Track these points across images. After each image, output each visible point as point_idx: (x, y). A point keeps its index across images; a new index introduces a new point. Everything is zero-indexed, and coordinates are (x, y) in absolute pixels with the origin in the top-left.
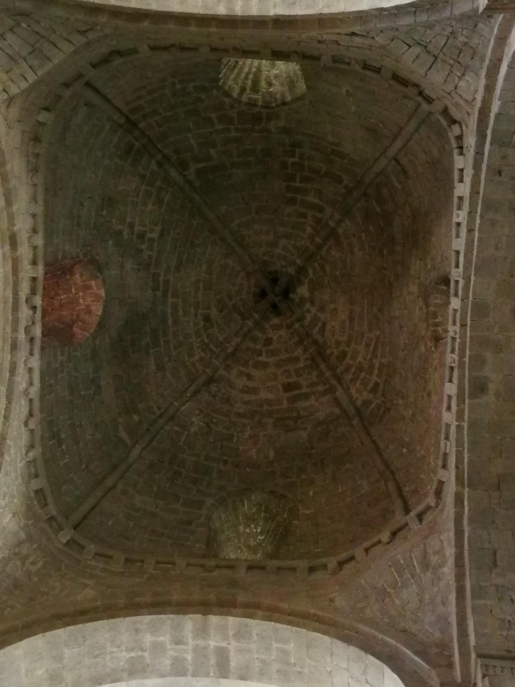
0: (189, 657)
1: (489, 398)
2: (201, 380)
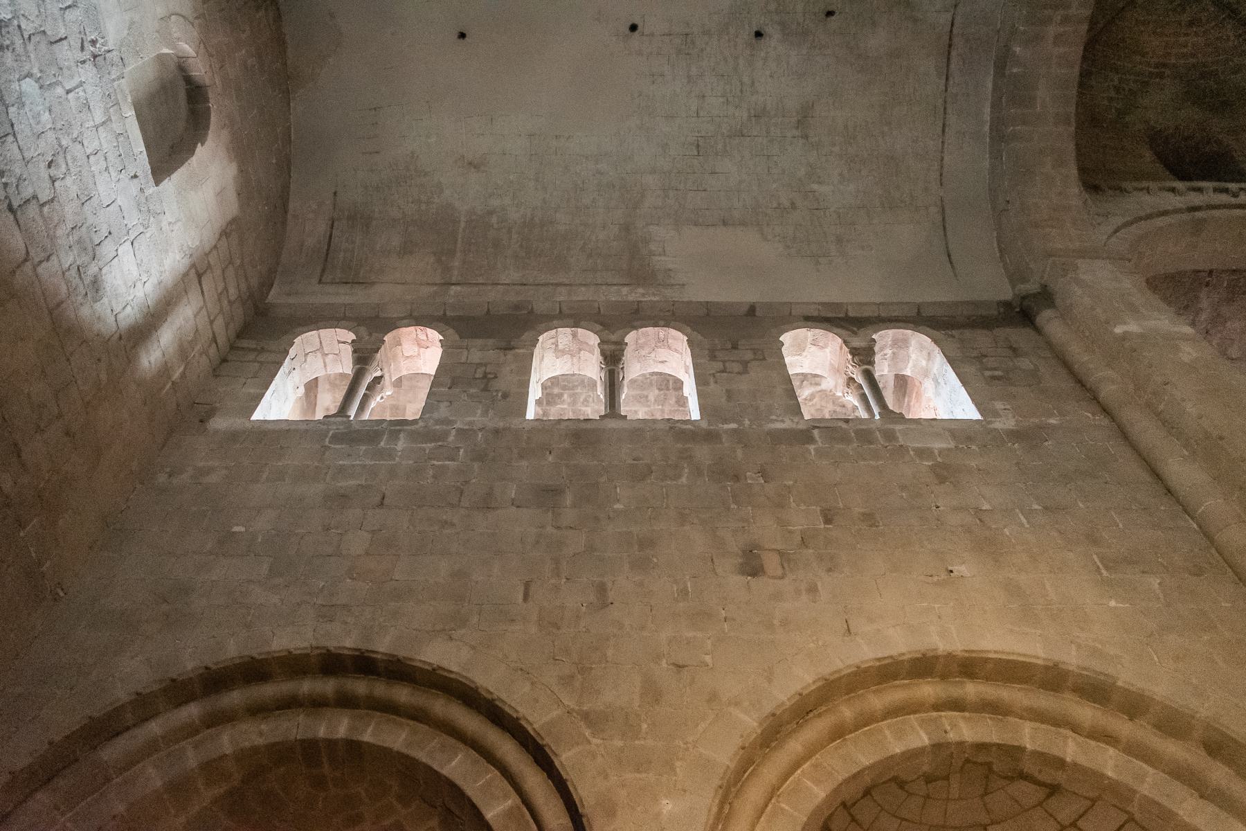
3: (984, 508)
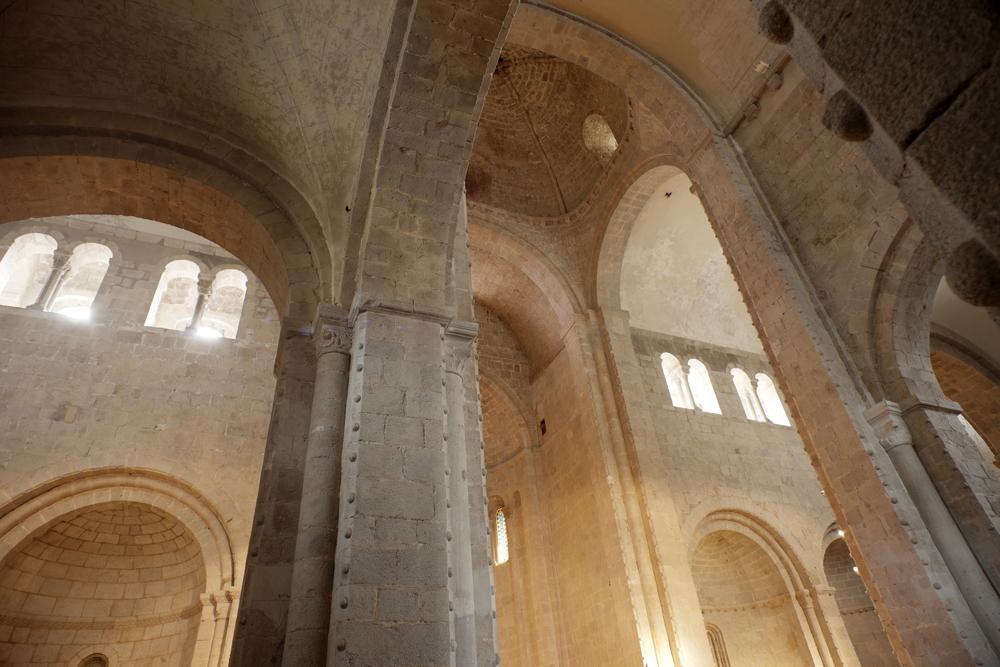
1: (590, 58)
2: (526, 118)
3: (313, 332)
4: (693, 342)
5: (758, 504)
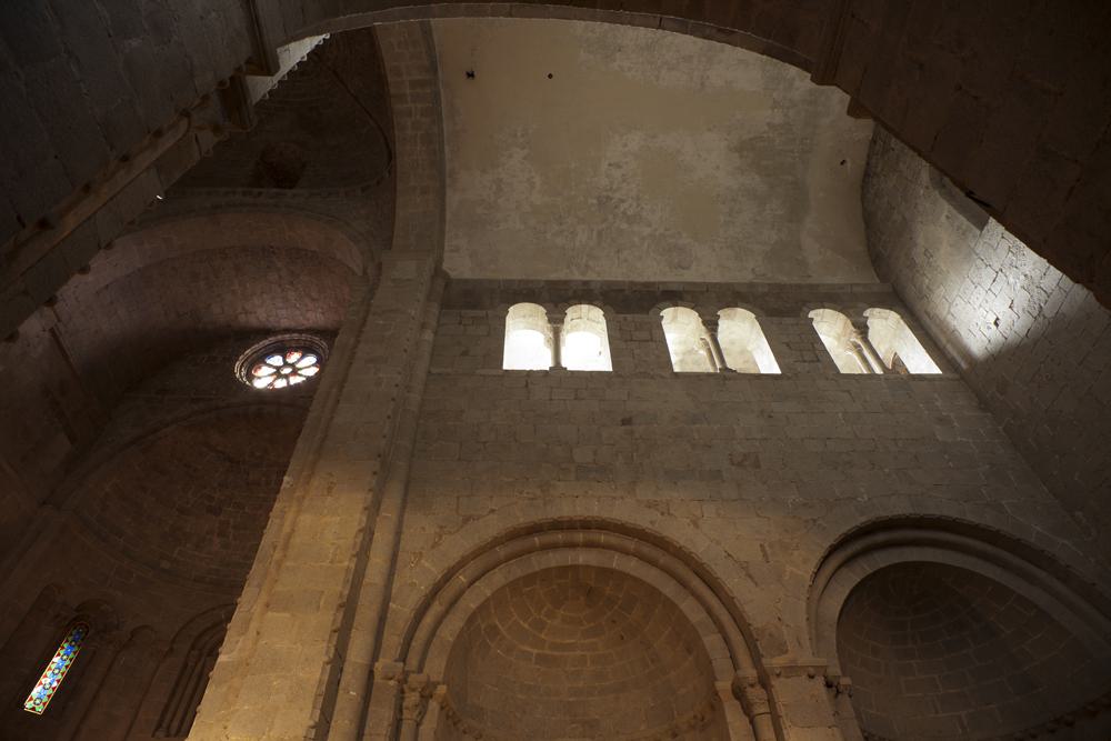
0: (419, 106)
4: (585, 283)
5: (651, 505)
